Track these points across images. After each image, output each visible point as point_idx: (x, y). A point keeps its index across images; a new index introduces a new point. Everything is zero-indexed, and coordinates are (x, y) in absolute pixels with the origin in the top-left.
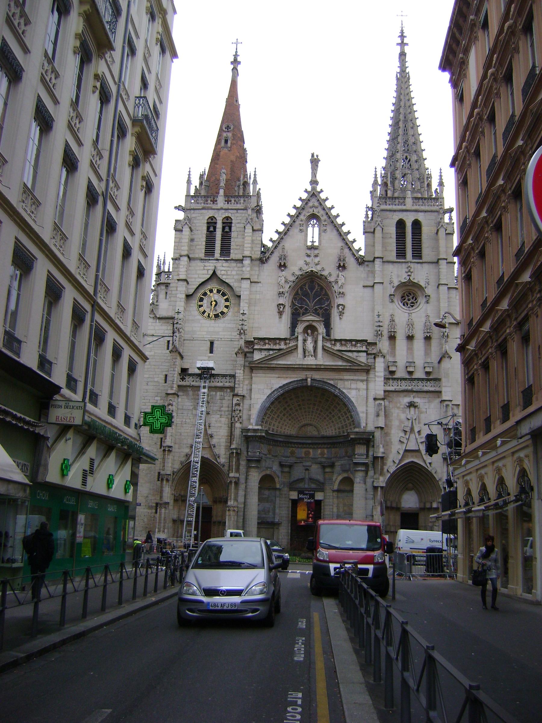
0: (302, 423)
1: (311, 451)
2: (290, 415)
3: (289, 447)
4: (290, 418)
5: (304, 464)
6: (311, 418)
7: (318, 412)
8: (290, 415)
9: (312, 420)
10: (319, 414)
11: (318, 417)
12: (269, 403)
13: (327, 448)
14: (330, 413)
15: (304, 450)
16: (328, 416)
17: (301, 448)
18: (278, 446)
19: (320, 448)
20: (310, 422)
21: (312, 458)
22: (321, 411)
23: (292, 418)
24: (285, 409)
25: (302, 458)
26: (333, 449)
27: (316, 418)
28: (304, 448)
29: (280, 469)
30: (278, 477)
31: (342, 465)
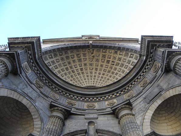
5: (86, 116)
7: (101, 76)
9: (95, 83)
10: (102, 77)
13: (116, 96)
15: (86, 104)
17: (83, 101)
18: (52, 89)
21: (98, 110)
22: (103, 74)
24: (67, 69)
25: (84, 110)
26: (124, 96)
27: (99, 81)
28: (87, 101)
29: (48, 113)
30: (42, 121)
31: (145, 98)
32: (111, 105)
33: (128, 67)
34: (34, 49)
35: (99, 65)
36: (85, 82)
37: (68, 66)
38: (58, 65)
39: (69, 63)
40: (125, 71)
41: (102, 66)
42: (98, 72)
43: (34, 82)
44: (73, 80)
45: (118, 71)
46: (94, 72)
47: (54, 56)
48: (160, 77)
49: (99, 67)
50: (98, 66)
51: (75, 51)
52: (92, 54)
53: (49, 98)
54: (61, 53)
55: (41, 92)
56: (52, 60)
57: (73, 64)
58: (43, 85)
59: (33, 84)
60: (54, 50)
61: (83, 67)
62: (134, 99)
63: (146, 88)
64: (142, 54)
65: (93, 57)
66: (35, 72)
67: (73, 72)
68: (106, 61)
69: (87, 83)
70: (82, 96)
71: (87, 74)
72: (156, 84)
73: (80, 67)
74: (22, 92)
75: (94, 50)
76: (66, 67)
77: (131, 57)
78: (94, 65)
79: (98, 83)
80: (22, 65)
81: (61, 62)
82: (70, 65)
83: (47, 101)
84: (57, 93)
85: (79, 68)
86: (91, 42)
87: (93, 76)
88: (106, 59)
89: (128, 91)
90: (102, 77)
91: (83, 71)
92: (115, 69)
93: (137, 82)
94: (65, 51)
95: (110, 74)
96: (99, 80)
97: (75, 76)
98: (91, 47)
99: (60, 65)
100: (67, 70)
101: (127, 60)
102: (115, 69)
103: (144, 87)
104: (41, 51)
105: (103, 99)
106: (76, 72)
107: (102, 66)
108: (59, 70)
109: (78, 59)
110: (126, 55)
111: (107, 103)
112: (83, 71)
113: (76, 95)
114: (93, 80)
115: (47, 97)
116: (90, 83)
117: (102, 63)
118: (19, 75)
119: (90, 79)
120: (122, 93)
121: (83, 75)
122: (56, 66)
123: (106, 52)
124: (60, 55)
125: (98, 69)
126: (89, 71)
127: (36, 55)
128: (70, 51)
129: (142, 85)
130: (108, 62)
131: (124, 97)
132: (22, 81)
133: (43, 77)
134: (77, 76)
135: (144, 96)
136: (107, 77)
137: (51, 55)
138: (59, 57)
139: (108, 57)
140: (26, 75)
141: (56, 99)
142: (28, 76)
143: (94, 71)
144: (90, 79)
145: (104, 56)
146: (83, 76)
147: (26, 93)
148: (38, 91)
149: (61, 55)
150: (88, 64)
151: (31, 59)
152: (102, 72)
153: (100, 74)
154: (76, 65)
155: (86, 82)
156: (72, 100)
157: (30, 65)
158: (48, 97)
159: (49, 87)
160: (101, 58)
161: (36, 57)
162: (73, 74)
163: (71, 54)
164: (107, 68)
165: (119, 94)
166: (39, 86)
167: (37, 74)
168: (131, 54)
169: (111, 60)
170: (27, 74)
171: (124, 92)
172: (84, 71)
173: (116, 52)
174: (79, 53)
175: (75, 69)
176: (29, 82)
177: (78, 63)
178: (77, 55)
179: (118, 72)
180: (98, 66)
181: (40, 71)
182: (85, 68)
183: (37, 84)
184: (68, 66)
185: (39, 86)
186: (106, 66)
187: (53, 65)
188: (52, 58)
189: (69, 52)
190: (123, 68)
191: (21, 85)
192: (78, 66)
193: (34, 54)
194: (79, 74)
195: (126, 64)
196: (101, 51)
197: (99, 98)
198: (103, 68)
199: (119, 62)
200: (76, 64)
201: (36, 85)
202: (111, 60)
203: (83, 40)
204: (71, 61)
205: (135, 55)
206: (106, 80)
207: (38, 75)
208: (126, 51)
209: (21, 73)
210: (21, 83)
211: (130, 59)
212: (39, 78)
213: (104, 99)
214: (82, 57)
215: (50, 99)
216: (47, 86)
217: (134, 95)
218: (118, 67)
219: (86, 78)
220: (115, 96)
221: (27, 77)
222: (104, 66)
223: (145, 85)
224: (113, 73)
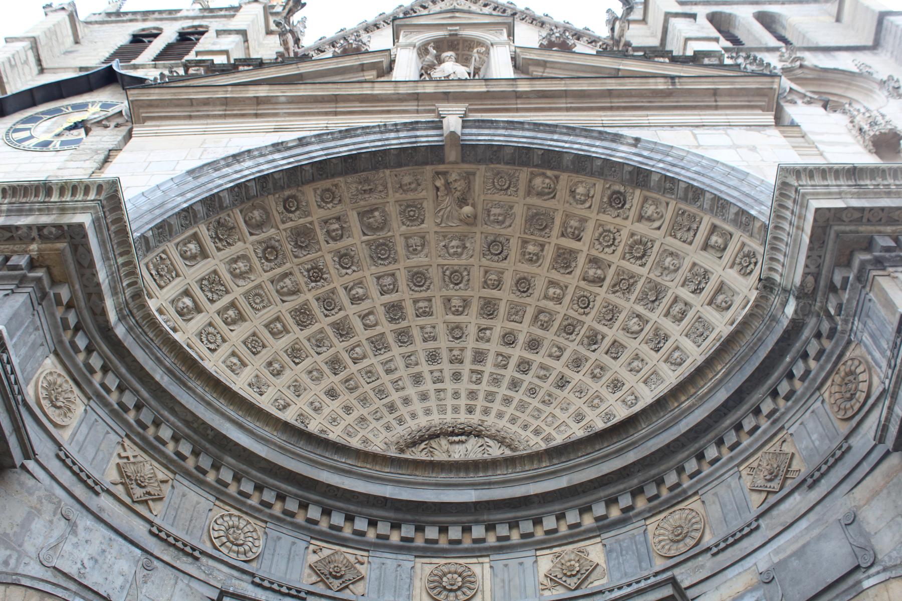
0: (413, 425)
1: (482, 570)
2: (335, 364)
3: (310, 530)
4: (331, 380)
6: (472, 394)
7: (517, 353)
8: (335, 364)
9: (480, 403)
10: (524, 366)
11: (514, 385)
12: (194, 195)
13: (604, 526)
14: (593, 339)
15: (425, 568)
16: (577, 363)
17: (406, 547)
18: (219, 492)
19: (552, 540)
20: (463, 418)
22: (534, 345)
23: (350, 385)
24: (303, 316)
27: (503, 390)
28: (430, 550)
32: (573, 582)
33: (691, 314)
34: (86, 266)
35: (508, 281)
36: (415, 399)
37: (309, 296)
38: (246, 295)
39: (316, 274)
40: (666, 338)
41: (523, 285)
42: (499, 326)
43: (112, 475)
44: (340, 388)
45: (626, 329)
46: (472, 330)
47: (216, 238)
48: (866, 466)
49: (505, 296)
50: (498, 285)
51: (346, 185)
52: (462, 201)
53: (204, 559)
54: (256, 214)
55: (157, 534)
56: (203, 268)
57: (337, 280)
58: (162, 474)
59: (108, 491)
60: (212, 203)
61: (405, 294)
62: (708, 564)
63: (783, 507)
64: (777, 277)
65: (471, 221)
66: (106, 404)
67: (343, 330)
68: (549, 253)
69: (432, 403)
70: (400, 516)
71: (431, 345)
72: (841, 504)
73: (387, 298)
74: (49, 575)
75: (474, 174)
76: (295, 302)
77: (713, 247)
78: (477, 275)
79: (496, 406)
80: (30, 393)
81: (262, 276)
82: (323, 289)
83: (195, 584)
84: (250, 512)
85: (377, 301)
86: (453, 123)
87: (468, 355)
88: (555, 240)
89: (679, 496)
90: (524, 366)
91: (404, 324)
92: (610, 314)
93: (732, 448)
94: (287, 193)
95: (572, 347)
96: (505, 383)
97: (355, 361)
98: (452, 155)
99: (256, 296)
100: (302, 325)
101: (687, 265)
102: (610, 314)
103: (773, 499)
104: (123, 231)
105: (523, 536)
106: (362, 334)
107: (523, 285)
108: (254, 334)
109: (368, 243)
110: (683, 226)
111: (546, 562)
112: (404, 324)
113: (365, 510)
114: (465, 386)
115: (192, 553)
116: (450, 402)
117: (526, 268)
118: (23, 467)
119: (447, 375)
120: (641, 504)
121: (404, 350)
122: (233, 305)
123: (551, 193)
124: (255, 227)
125: (503, 308)
126: (440, 319)
127: (101, 299)
128: (315, 190)
129: (760, 482)
130: (565, 260)
131: (650, 536)
132: (40, 500)
133: (157, 424)
134: (365, 363)
135: (763, 560)
136: (558, 367)
137: (195, 237)
138: (246, 245)
139: (564, 225)
140: (59, 446)
141: (251, 556)
142: (72, 450)
143: (472, 320)
144: (447, 375)
145: (539, 222)
146: (407, 357)
147: (72, 570)
148: (139, 530)
149: (260, 226)
150: (435, 274)
151: (77, 328)
152: (524, 330)
153: (509, 339)
154: (360, 283)
155: (424, 397)
156: (343, 542)
157: (75, 365)
158: (203, 553)
159: (201, 483)
160: (514, 231)
161: (104, 313)
162: (340, 347)
163: (322, 213)
164: (559, 300)
165: (625, 510)
166: (138, 492)
167: (118, 413)
168: (714, 228)
169: (583, 247)
170: (64, 436)
171: (650, 500)
172: (412, 321)
173: (617, 201)
174: (373, 199)
175: (351, 311)
176: (79, 491)
177: (368, 272)
178: (361, 215)
179: (622, 337)
180: (498, 285)
181: (136, 392)
182: (415, 301)
183: (125, 479)
184: (309, 296)
185: (138, 492)
186: (551, 291)
187: (212, 301)
188: (204, 254)
189: (310, 194)
190: (656, 317)
191: (38, 525)
192: (374, 291)
193: (89, 295)
194: (379, 344)
195: (675, 288)
196: (522, 186)
197: (503, 530)
198: (532, 303)
199: (634, 268)
200: (356, 276)
201: (119, 491)
202: (583, 247)
203: (403, 90)
204: (329, 258)
205: (739, 237)
206: (547, 386)
207: (131, 417)
208: (685, 199)
209: (28, 452)
210: (34, 512)
211: (707, 260)
212: (138, 434)
213: (531, 535)
214: (398, 229)
215: (211, 562)
216: (187, 474)
217: (708, 540)
218: (628, 304)
219: (424, 368)
220: (597, 519)
221: (65, 459)
222: (539, 285)
223: (775, 485)
224: (593, 339)
